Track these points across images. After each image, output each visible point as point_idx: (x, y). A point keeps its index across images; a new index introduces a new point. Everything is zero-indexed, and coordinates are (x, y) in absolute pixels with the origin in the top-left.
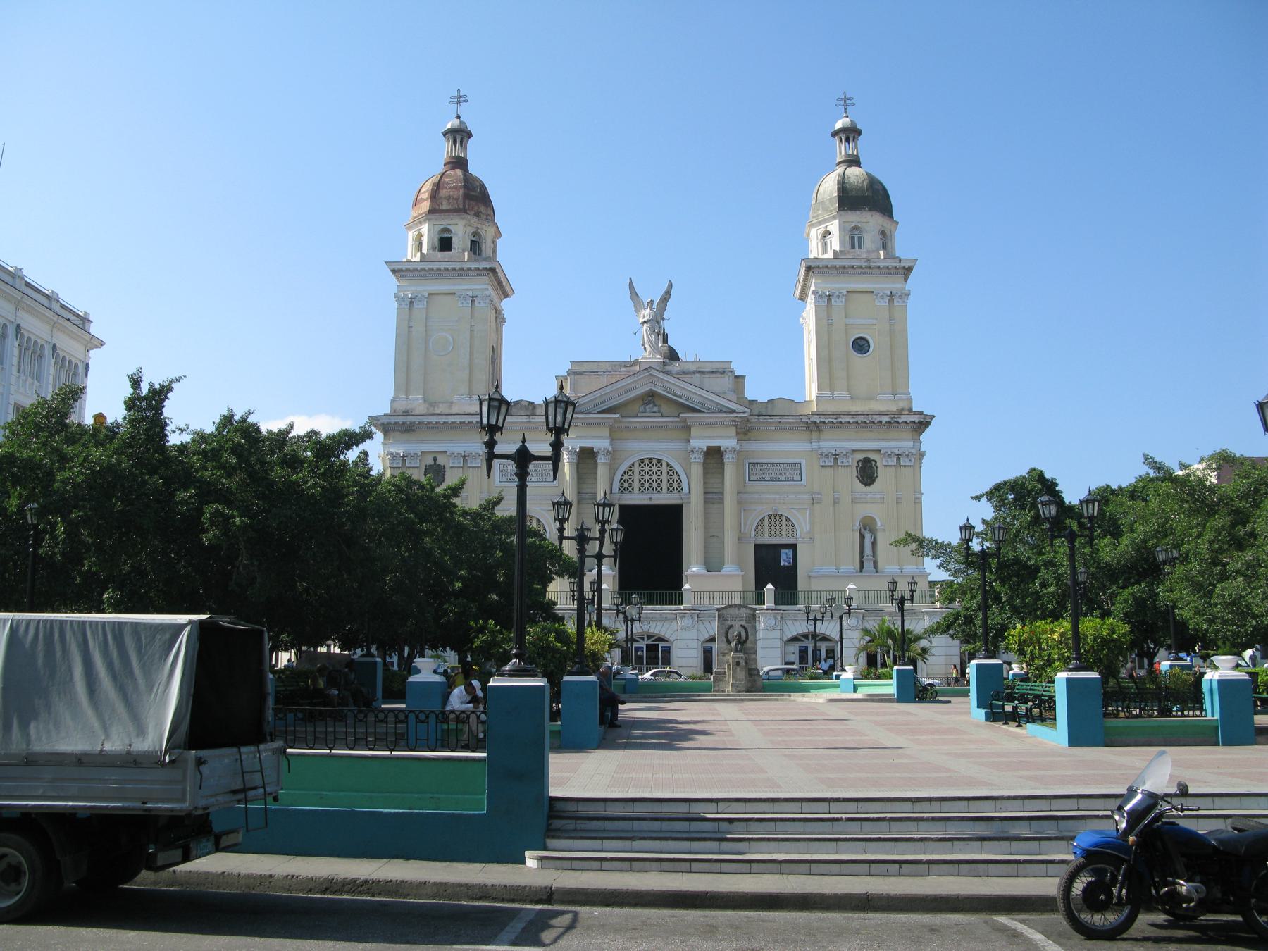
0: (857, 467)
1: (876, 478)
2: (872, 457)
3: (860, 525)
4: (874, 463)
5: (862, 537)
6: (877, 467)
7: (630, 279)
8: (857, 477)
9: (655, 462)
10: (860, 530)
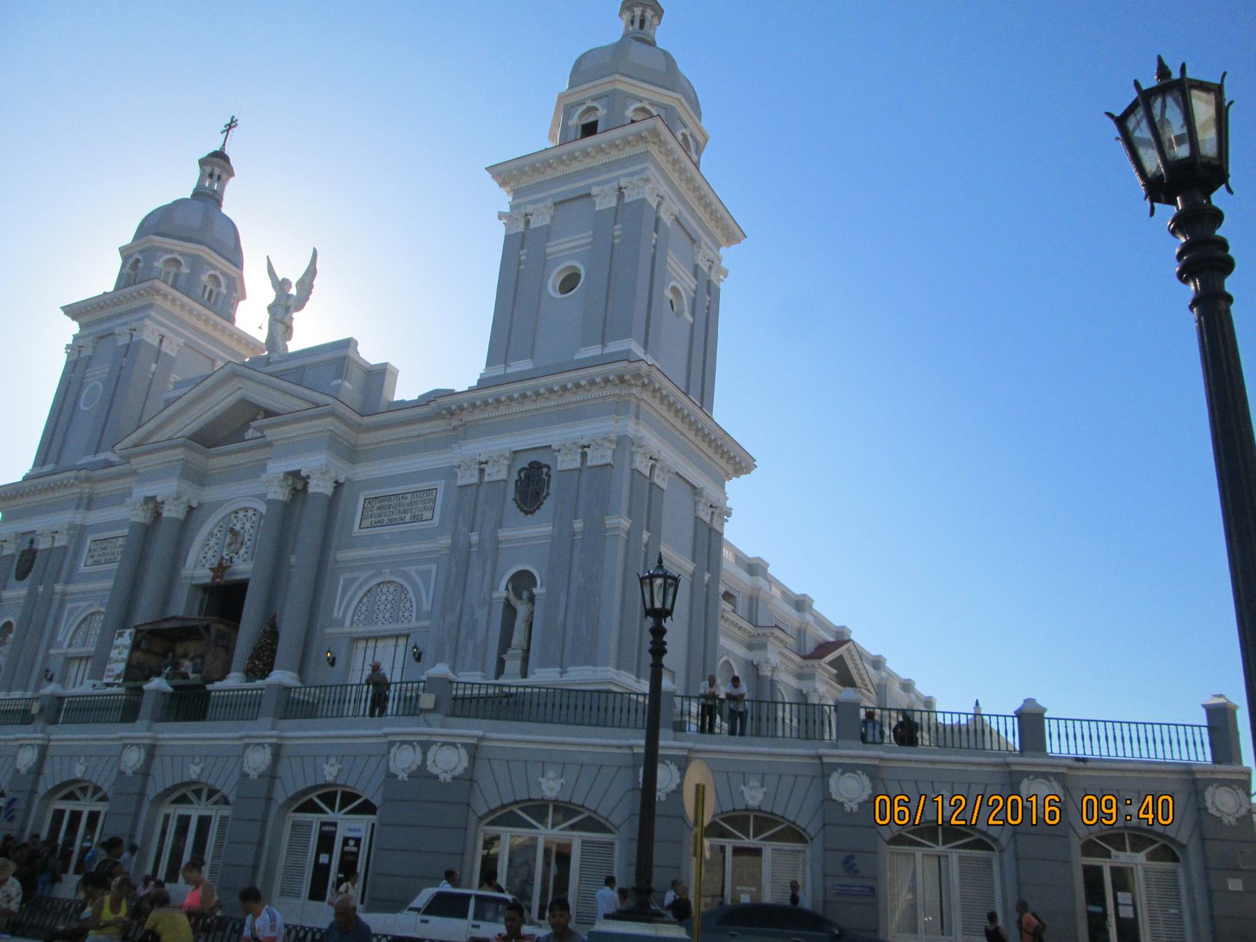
0: (517, 481)
1: (545, 498)
2: (543, 458)
3: (507, 589)
4: (545, 470)
5: (510, 611)
6: (549, 476)
7: (268, 257)
8: (515, 499)
9: (250, 513)
10: (507, 599)
